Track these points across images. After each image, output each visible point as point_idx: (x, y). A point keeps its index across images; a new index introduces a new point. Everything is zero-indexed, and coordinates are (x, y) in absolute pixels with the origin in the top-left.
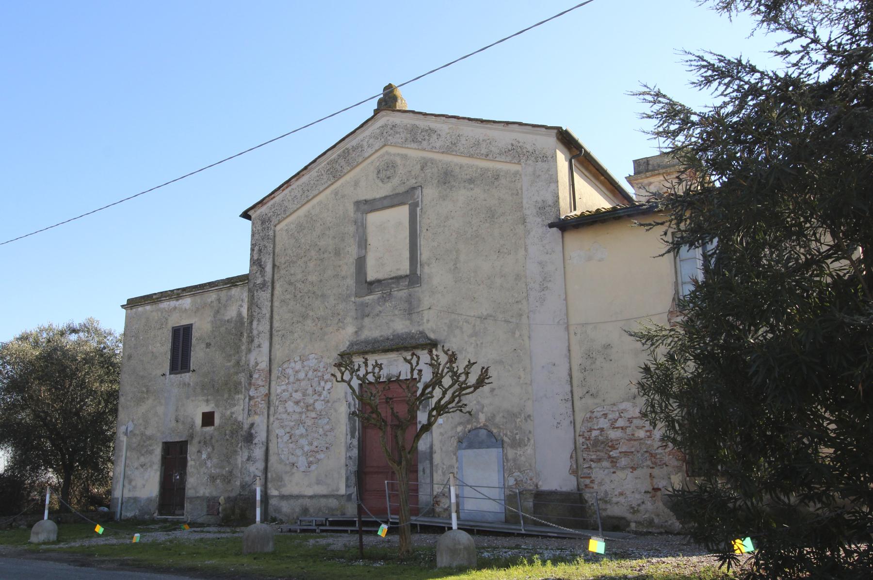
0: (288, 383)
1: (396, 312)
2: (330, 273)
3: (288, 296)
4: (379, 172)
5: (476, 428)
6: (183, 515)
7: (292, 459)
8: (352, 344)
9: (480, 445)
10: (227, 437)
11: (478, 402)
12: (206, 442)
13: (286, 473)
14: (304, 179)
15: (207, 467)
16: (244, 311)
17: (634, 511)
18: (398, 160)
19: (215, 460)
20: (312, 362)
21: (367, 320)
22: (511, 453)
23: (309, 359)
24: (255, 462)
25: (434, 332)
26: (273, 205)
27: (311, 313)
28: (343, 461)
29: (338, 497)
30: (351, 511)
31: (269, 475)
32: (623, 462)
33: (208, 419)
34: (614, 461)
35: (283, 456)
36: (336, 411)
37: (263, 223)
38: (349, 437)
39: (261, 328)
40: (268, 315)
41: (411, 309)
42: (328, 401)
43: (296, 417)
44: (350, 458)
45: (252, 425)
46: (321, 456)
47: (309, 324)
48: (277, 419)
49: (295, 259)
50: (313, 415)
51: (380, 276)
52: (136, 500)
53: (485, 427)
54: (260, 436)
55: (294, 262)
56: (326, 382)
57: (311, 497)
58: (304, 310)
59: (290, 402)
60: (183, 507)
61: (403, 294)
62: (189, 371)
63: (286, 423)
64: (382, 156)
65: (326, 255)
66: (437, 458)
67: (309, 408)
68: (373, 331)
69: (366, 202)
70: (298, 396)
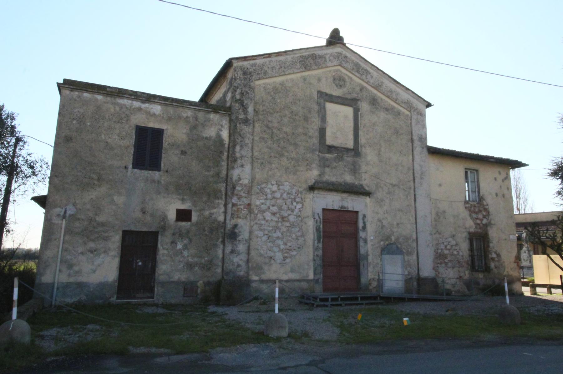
0: (266, 199)
1: (346, 169)
2: (300, 130)
3: (266, 136)
4: (334, 79)
5: (391, 244)
6: (153, 298)
7: (270, 254)
8: (316, 182)
9: (393, 253)
10: (207, 232)
11: (391, 230)
12: (181, 235)
13: (266, 264)
14: (282, 58)
15: (183, 256)
16: (225, 134)
17: (454, 285)
18: (346, 78)
19: (192, 251)
20: (286, 187)
21: (327, 170)
22: (406, 258)
23: (283, 185)
24: (238, 254)
25: (368, 187)
26: (255, 65)
27: (286, 154)
28: (311, 257)
29: (308, 281)
30: (319, 290)
31: (250, 265)
32: (450, 264)
33: (183, 215)
34: (446, 264)
35: (262, 252)
36: (305, 223)
37: (245, 73)
38: (316, 242)
39: (244, 153)
40: (250, 145)
41: (355, 170)
42: (299, 216)
43: (274, 224)
44: (317, 256)
45: (236, 226)
46: (294, 253)
47: (284, 161)
48: (256, 223)
49: (271, 111)
50: (288, 224)
51: (335, 144)
52: (80, 285)
53: (394, 243)
54: (244, 235)
55: (271, 113)
56: (297, 203)
57: (287, 281)
58: (280, 149)
59: (267, 213)
60: (152, 290)
61: (350, 159)
62: (159, 170)
63: (266, 228)
64: (337, 71)
65: (297, 118)
66: (370, 259)
67: (285, 219)
68: (330, 177)
69: (327, 94)
70: (275, 209)
